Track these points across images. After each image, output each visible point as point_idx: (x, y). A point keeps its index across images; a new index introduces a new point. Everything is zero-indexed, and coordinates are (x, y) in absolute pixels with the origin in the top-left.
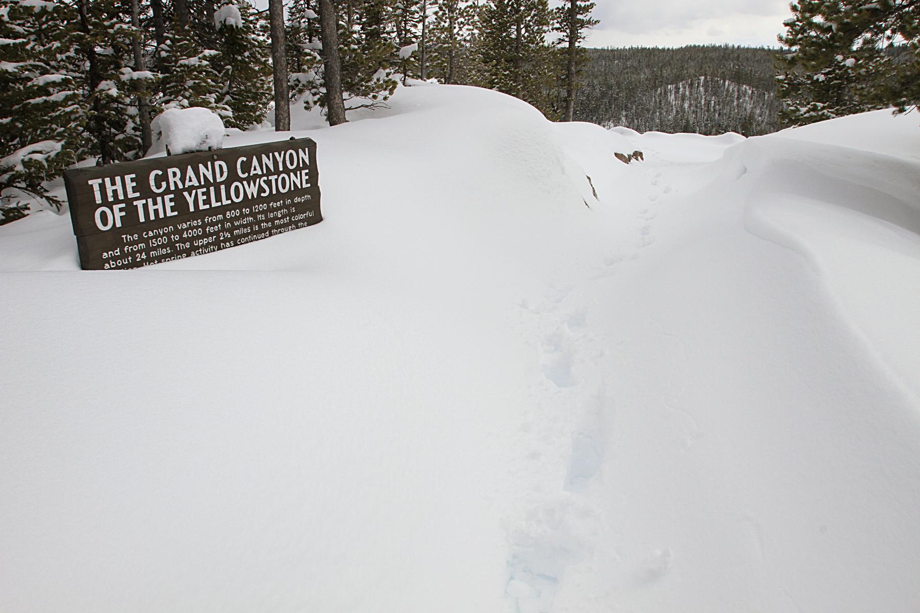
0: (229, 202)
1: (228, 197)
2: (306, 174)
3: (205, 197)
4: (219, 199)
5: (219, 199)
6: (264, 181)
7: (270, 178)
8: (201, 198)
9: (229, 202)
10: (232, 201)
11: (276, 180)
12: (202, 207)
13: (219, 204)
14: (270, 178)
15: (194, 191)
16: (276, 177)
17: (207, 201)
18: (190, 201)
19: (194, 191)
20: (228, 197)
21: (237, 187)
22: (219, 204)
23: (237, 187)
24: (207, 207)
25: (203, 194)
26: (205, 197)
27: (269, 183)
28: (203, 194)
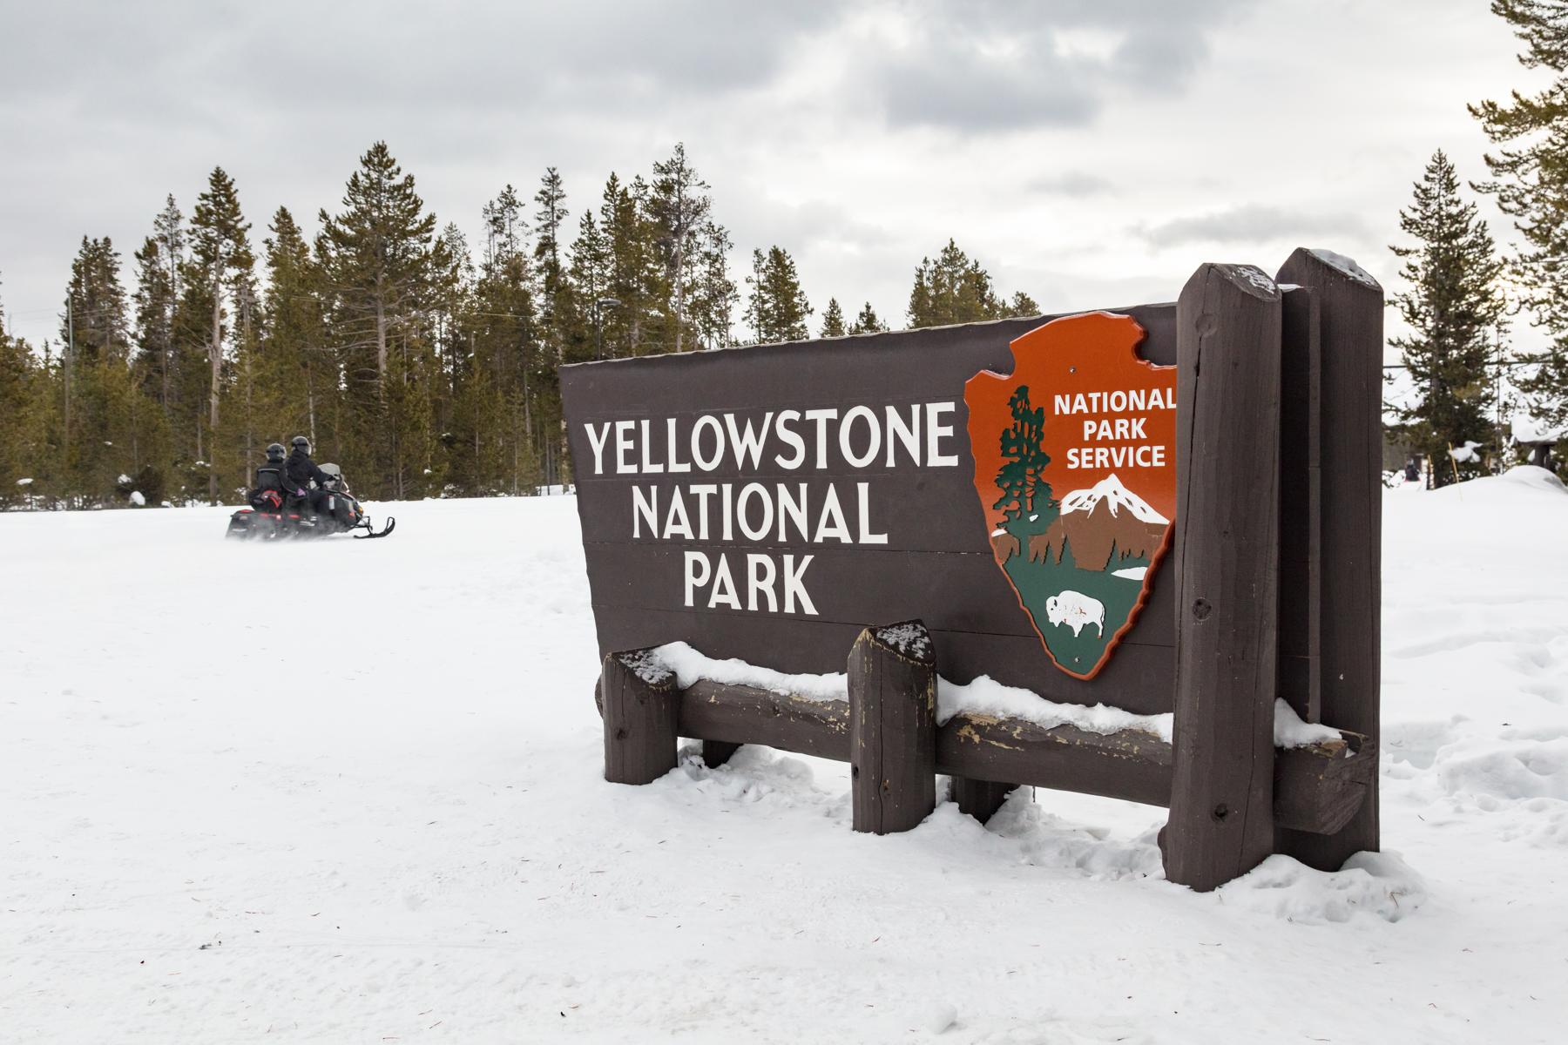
0: (686, 468)
1: (684, 455)
2: (943, 419)
3: (630, 445)
4: (659, 455)
5: (659, 455)
6: (789, 425)
7: (810, 415)
8: (623, 445)
9: (686, 468)
10: (694, 465)
11: (833, 426)
12: (623, 468)
13: (659, 469)
14: (810, 415)
15: (607, 426)
16: (833, 414)
17: (633, 457)
18: (598, 448)
19: (607, 426)
20: (684, 455)
21: (708, 429)
22: (659, 469)
23: (708, 429)
24: (633, 469)
25: (628, 435)
26: (630, 445)
27: (806, 429)
28: (628, 435)
